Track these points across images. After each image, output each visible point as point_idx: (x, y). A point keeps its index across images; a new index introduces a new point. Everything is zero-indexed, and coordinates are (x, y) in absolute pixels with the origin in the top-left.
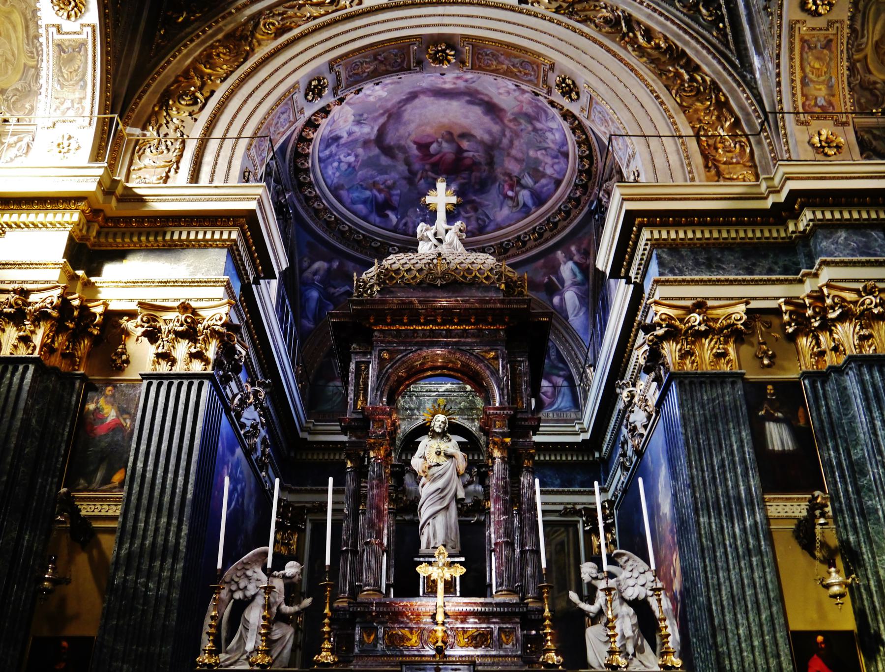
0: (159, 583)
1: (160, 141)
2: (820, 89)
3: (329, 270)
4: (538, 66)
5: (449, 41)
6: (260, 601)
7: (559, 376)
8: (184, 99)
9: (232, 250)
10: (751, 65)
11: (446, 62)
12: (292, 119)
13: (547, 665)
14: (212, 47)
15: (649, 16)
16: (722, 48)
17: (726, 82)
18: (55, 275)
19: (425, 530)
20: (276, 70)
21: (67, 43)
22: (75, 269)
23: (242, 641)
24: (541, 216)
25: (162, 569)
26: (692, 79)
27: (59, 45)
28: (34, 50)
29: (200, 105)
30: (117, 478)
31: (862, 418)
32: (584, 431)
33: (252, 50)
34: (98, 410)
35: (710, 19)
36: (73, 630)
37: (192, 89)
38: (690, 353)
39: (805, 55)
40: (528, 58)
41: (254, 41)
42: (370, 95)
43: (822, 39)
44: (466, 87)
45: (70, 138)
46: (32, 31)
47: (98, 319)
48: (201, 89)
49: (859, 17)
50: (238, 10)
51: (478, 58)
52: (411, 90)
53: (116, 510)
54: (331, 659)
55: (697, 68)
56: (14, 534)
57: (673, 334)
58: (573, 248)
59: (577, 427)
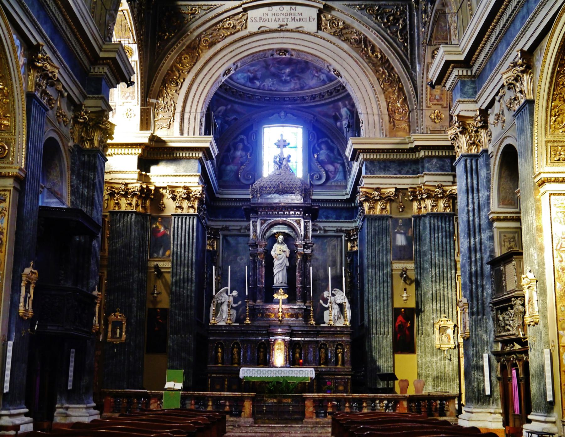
0: (187, 291)
3: (226, 110)
6: (226, 303)
7: (338, 163)
9: (200, 160)
10: (416, 68)
13: (310, 324)
14: (181, 54)
15: (375, 39)
16: (405, 57)
17: (403, 78)
18: (136, 176)
19: (276, 277)
22: (141, 171)
23: (221, 315)
24: (331, 86)
25: (187, 286)
26: (390, 75)
29: (180, 86)
30: (167, 253)
31: (428, 236)
32: (347, 194)
33: (199, 55)
34: (157, 227)
35: (401, 41)
36: (160, 306)
38: (373, 208)
47: (153, 192)
50: (191, 33)
53: (169, 265)
54: (249, 322)
55: (393, 68)
56: (137, 275)
57: (367, 200)
58: (347, 102)
59: (344, 193)
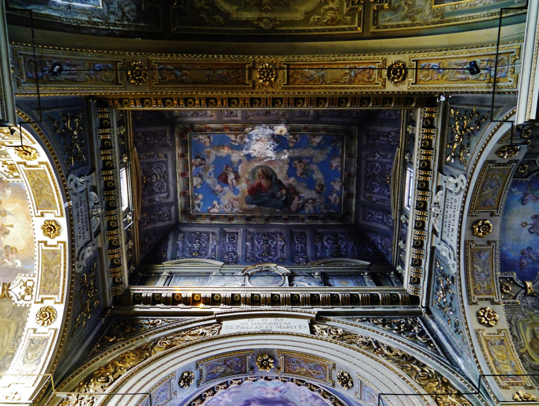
1: (77, 402)
2: (507, 368)
4: (325, 367)
5: (271, 354)
8: (100, 379)
11: (268, 368)
12: (168, 397)
14: (127, 353)
15: (388, 341)
17: (444, 372)
20: (163, 365)
21: (37, 339)
26: (423, 371)
27: (31, 340)
28: (16, 344)
29: (110, 382)
37: (108, 374)
39: (490, 349)
40: (319, 362)
41: (153, 351)
42: (220, 401)
43: (498, 340)
44: (281, 397)
45: (16, 393)
46: (19, 334)
48: (113, 374)
49: (514, 329)
51: (288, 365)
52: (247, 399)
55: (424, 365)
